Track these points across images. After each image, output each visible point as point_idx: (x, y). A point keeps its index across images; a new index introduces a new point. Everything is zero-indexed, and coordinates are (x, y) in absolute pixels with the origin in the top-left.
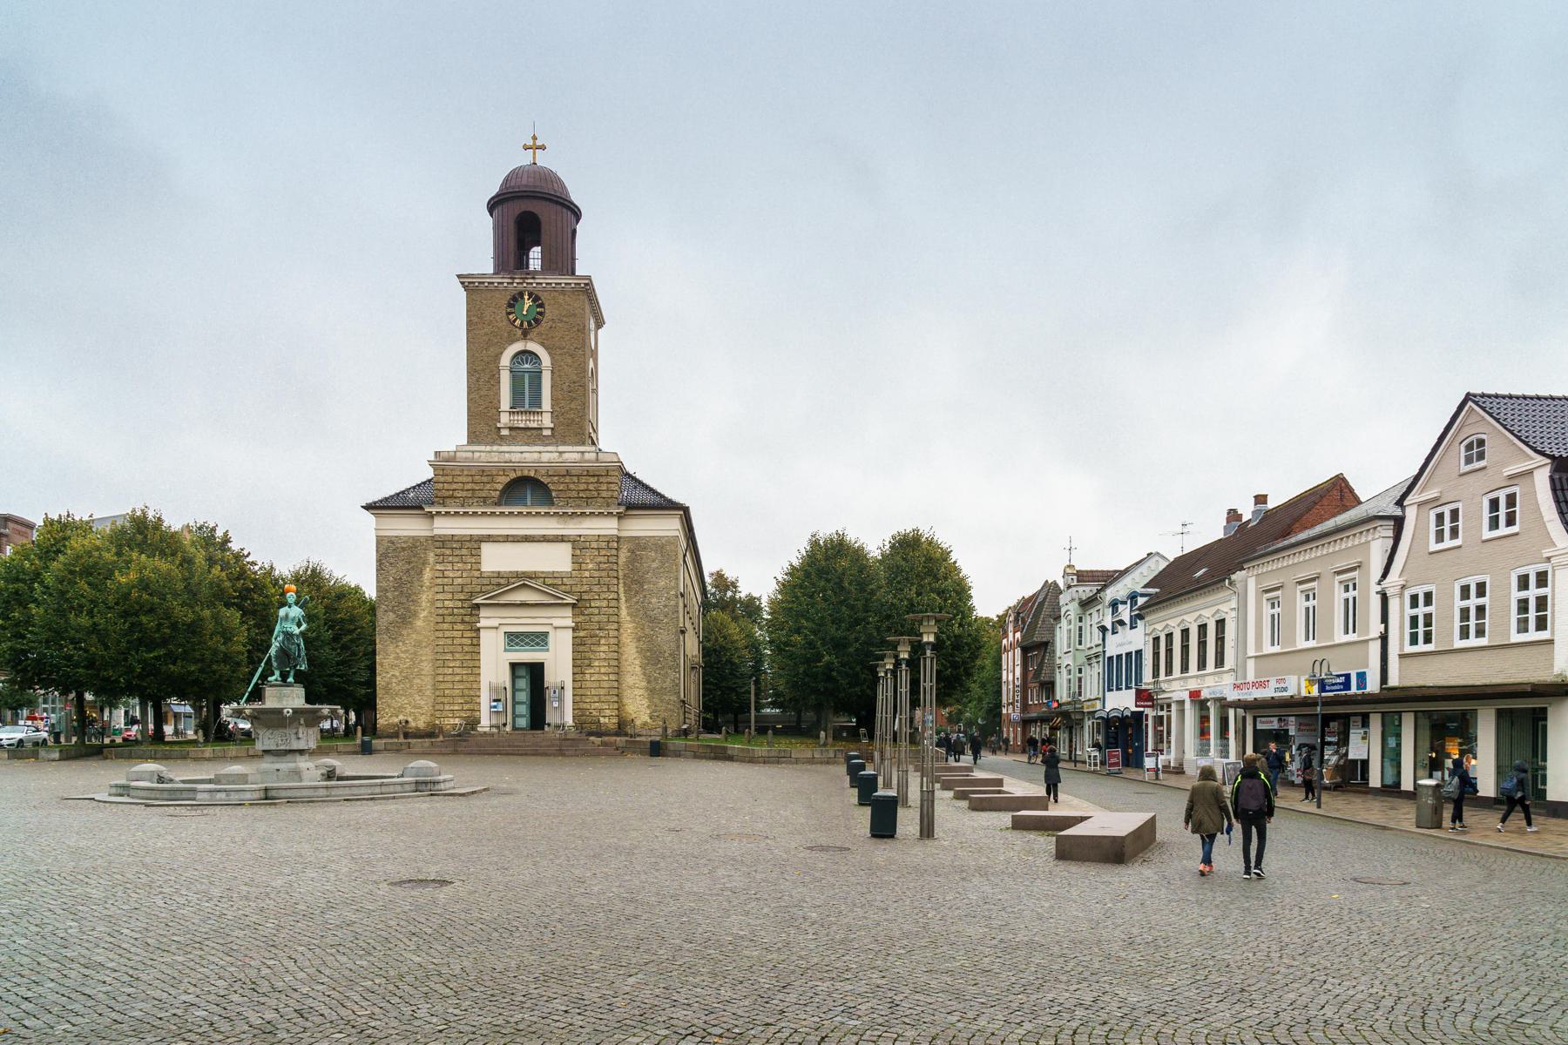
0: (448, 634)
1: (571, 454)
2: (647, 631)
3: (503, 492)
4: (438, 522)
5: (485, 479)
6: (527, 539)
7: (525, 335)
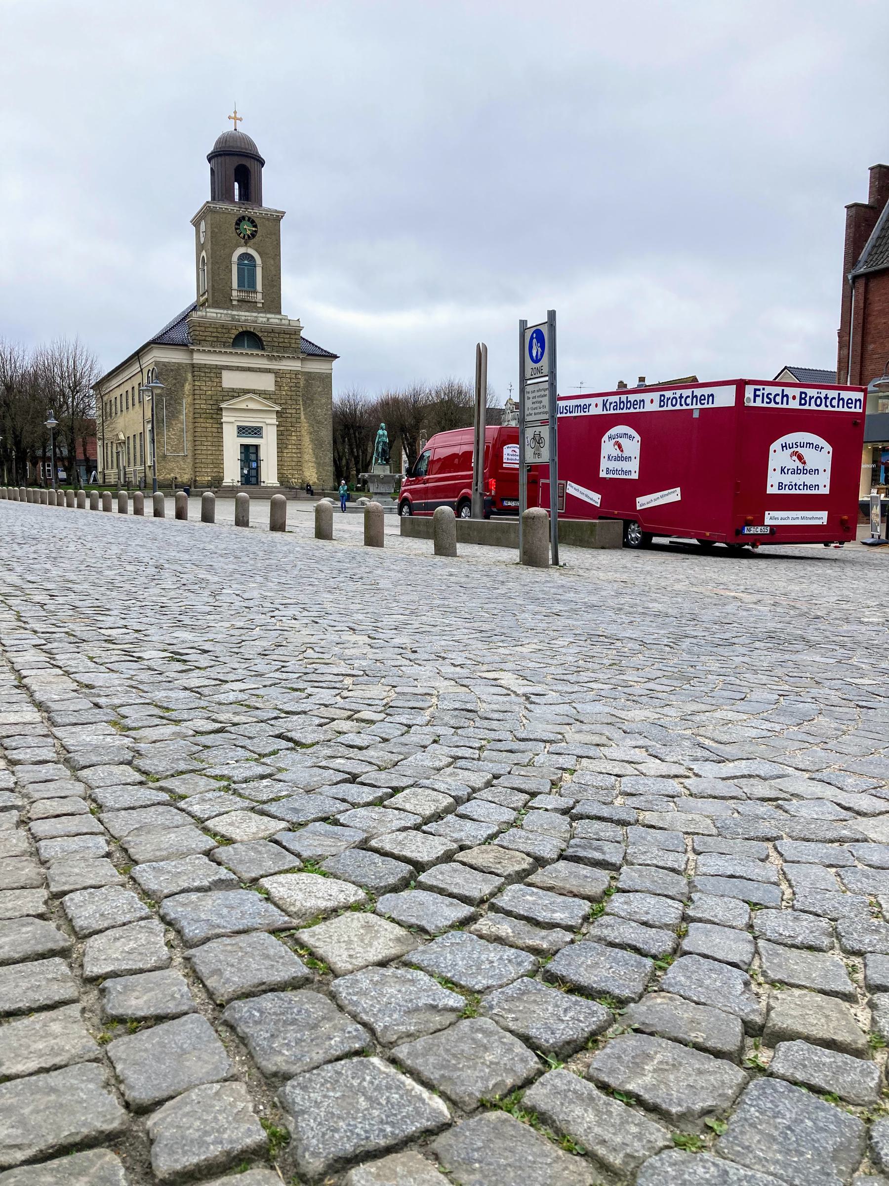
0: (203, 425)
1: (274, 319)
2: (316, 429)
3: (234, 339)
5: (224, 331)
7: (246, 243)
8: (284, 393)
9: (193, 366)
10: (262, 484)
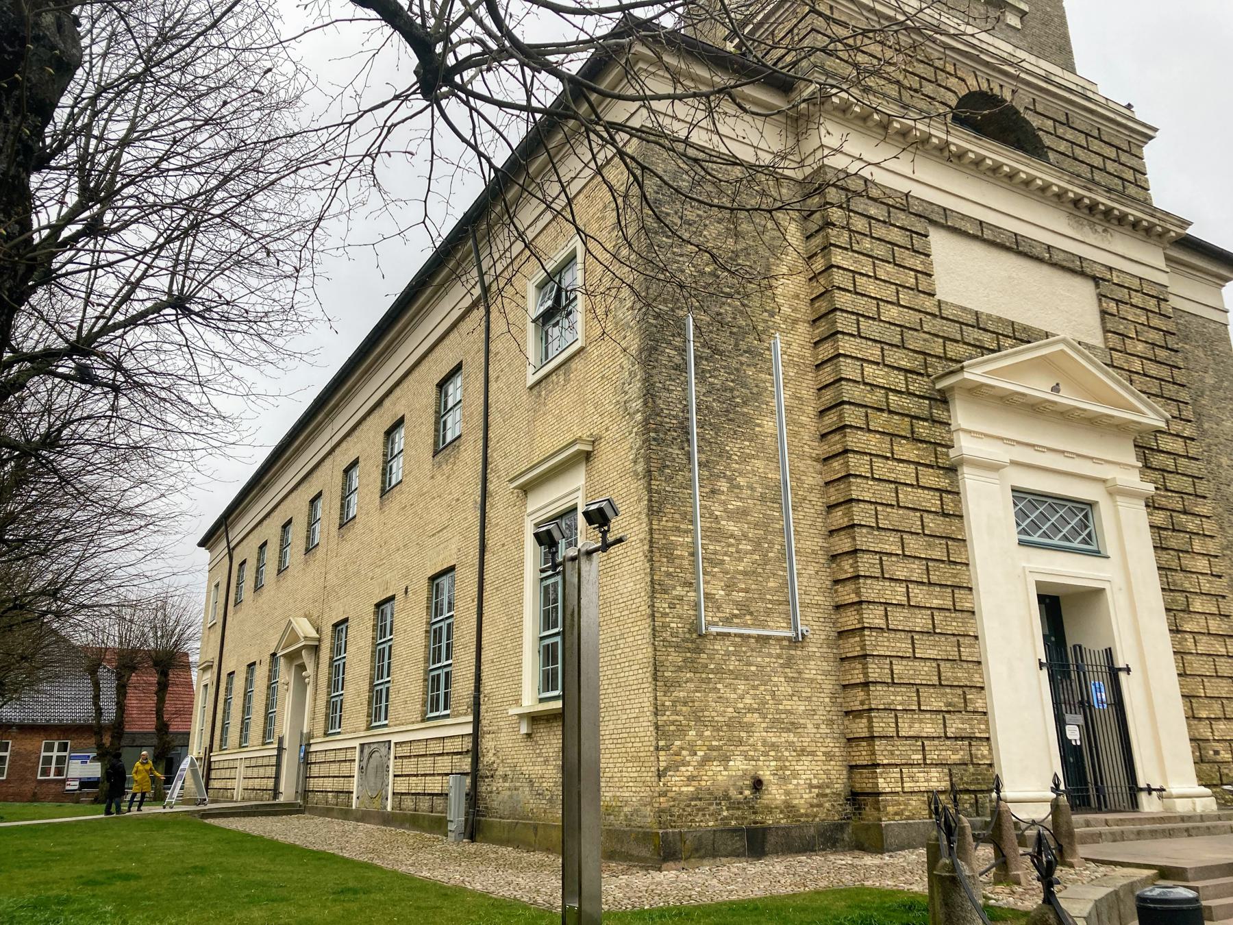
6: (1016, 247)
9: (815, 185)
10: (1150, 805)
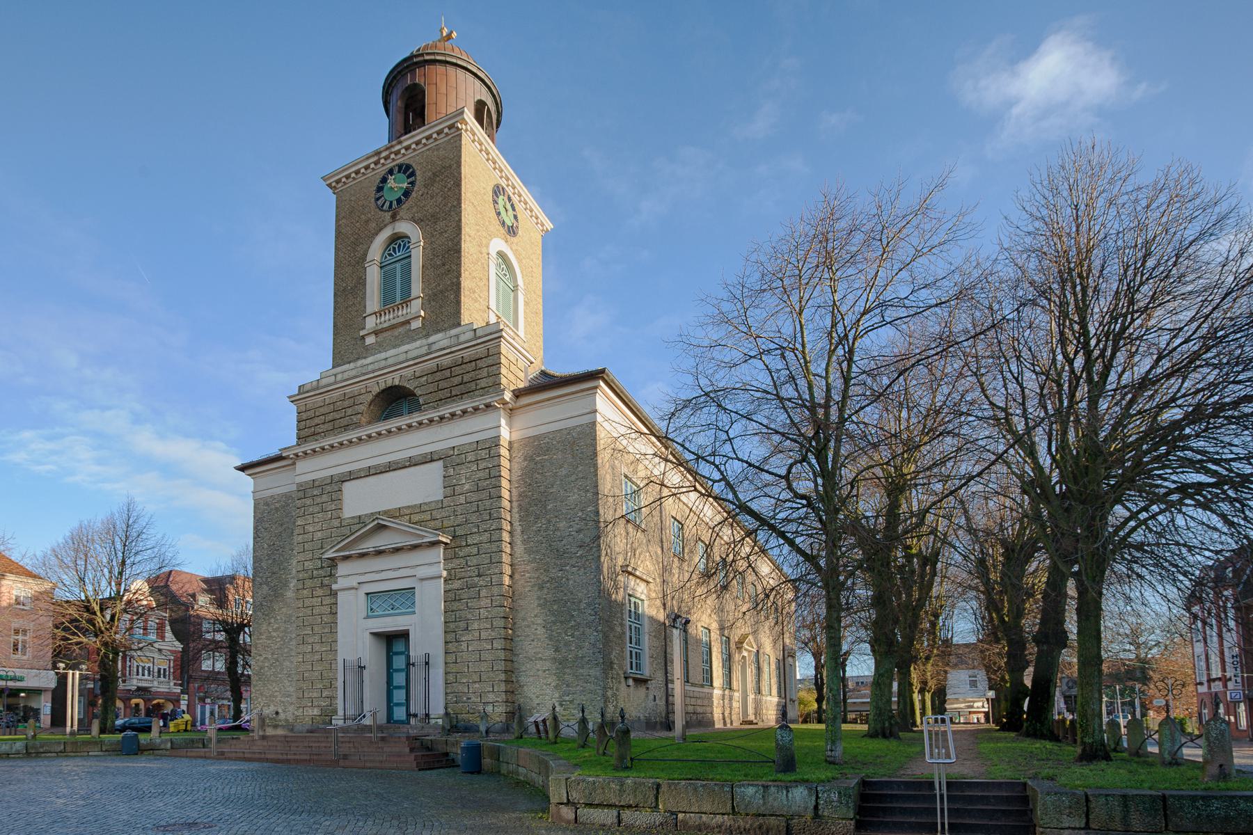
2: (555, 573)
4: (301, 466)
8: (462, 499)
